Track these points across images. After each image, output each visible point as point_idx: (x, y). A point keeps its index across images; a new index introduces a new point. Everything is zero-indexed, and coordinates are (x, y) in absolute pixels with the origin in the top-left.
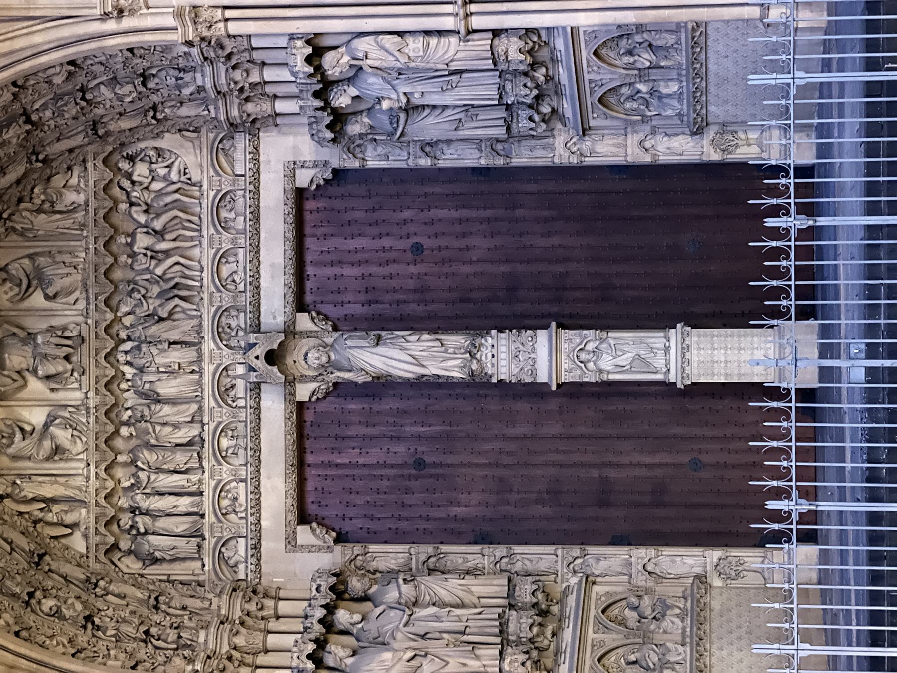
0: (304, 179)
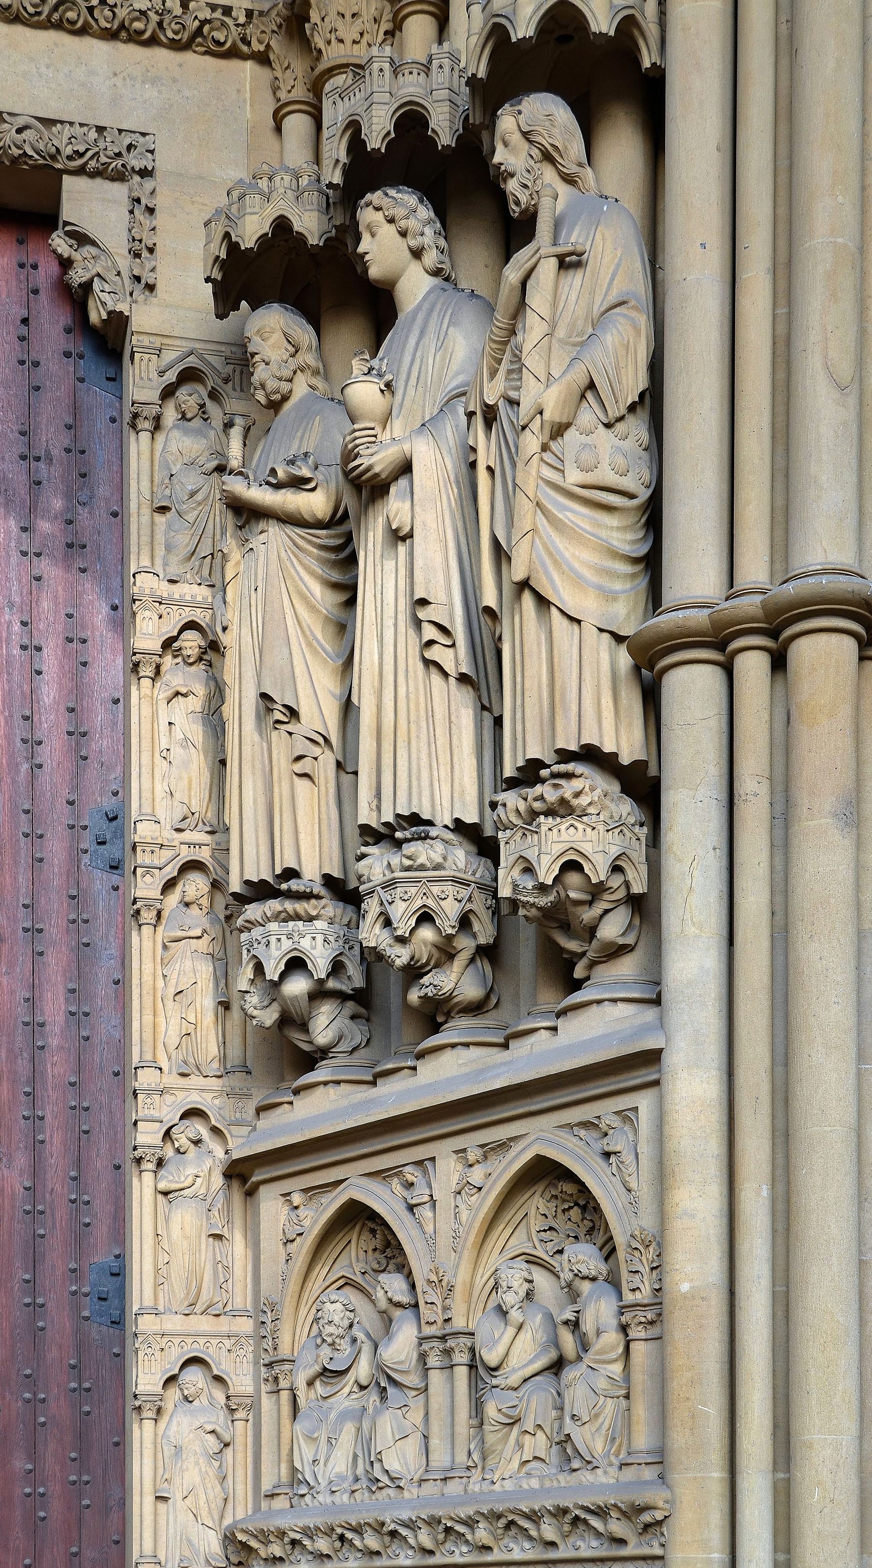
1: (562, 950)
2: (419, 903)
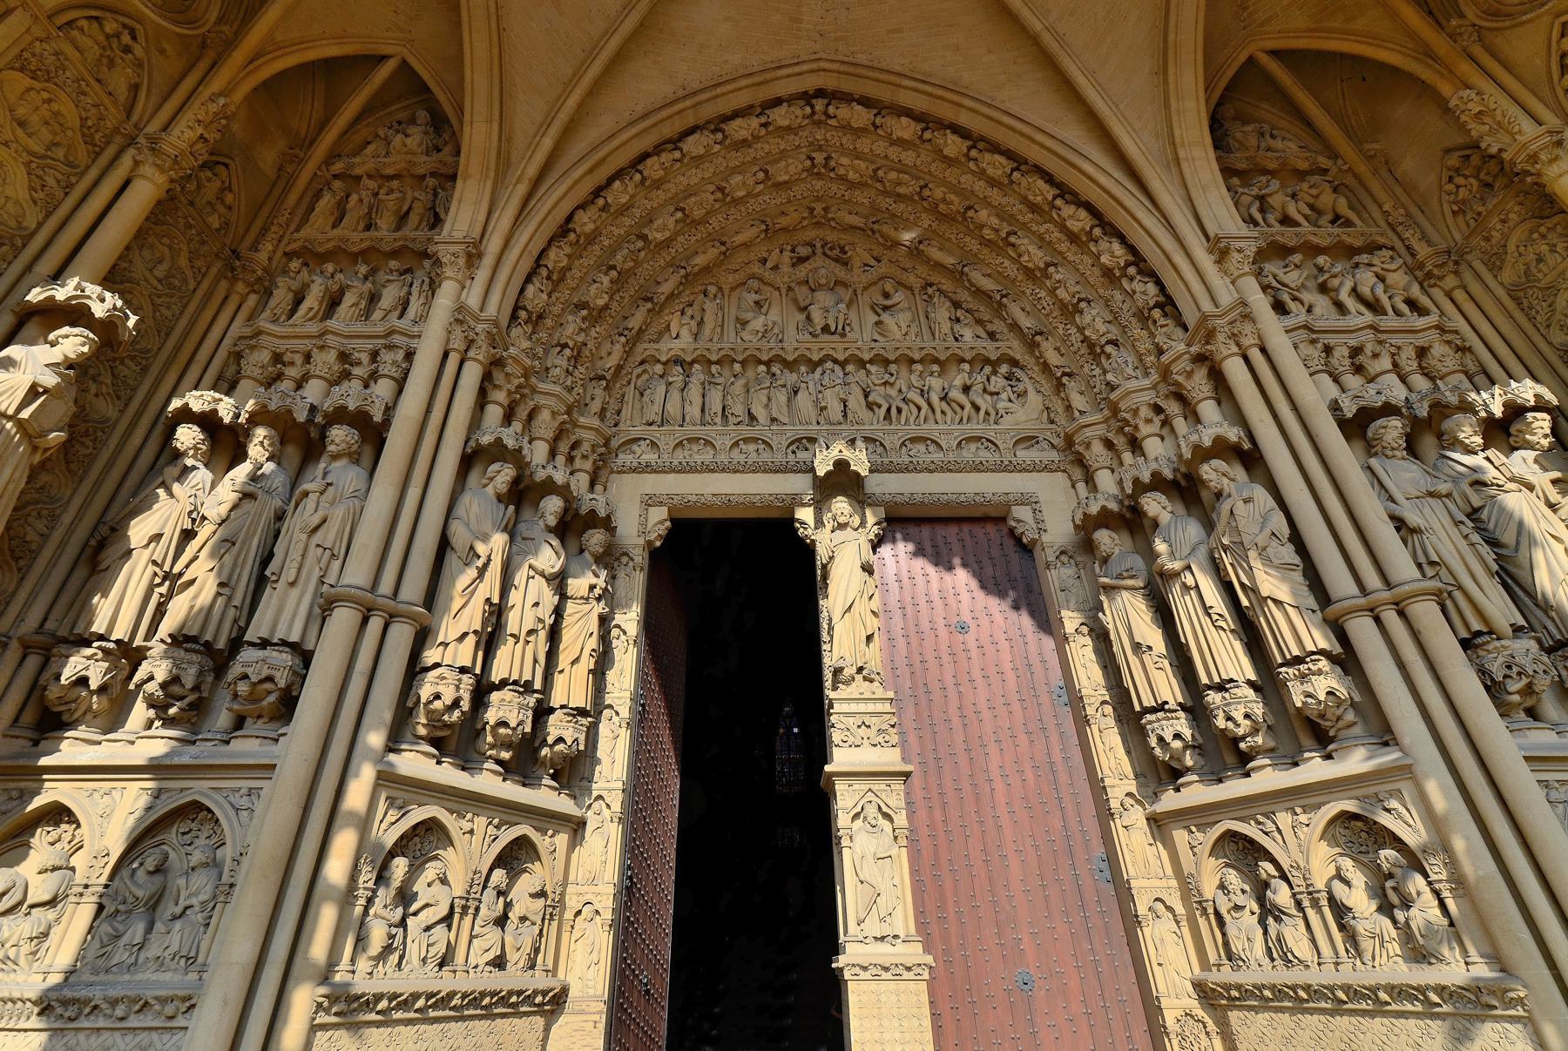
0: (1022, 513)
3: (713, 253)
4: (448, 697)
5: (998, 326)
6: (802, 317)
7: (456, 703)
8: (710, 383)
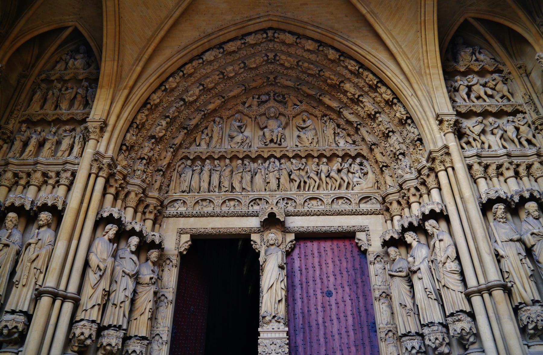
1: (463, 343)
2: (435, 337)
3: (218, 102)
4: (87, 333)
5: (357, 138)
6: (261, 133)
7: (90, 336)
8: (214, 170)
